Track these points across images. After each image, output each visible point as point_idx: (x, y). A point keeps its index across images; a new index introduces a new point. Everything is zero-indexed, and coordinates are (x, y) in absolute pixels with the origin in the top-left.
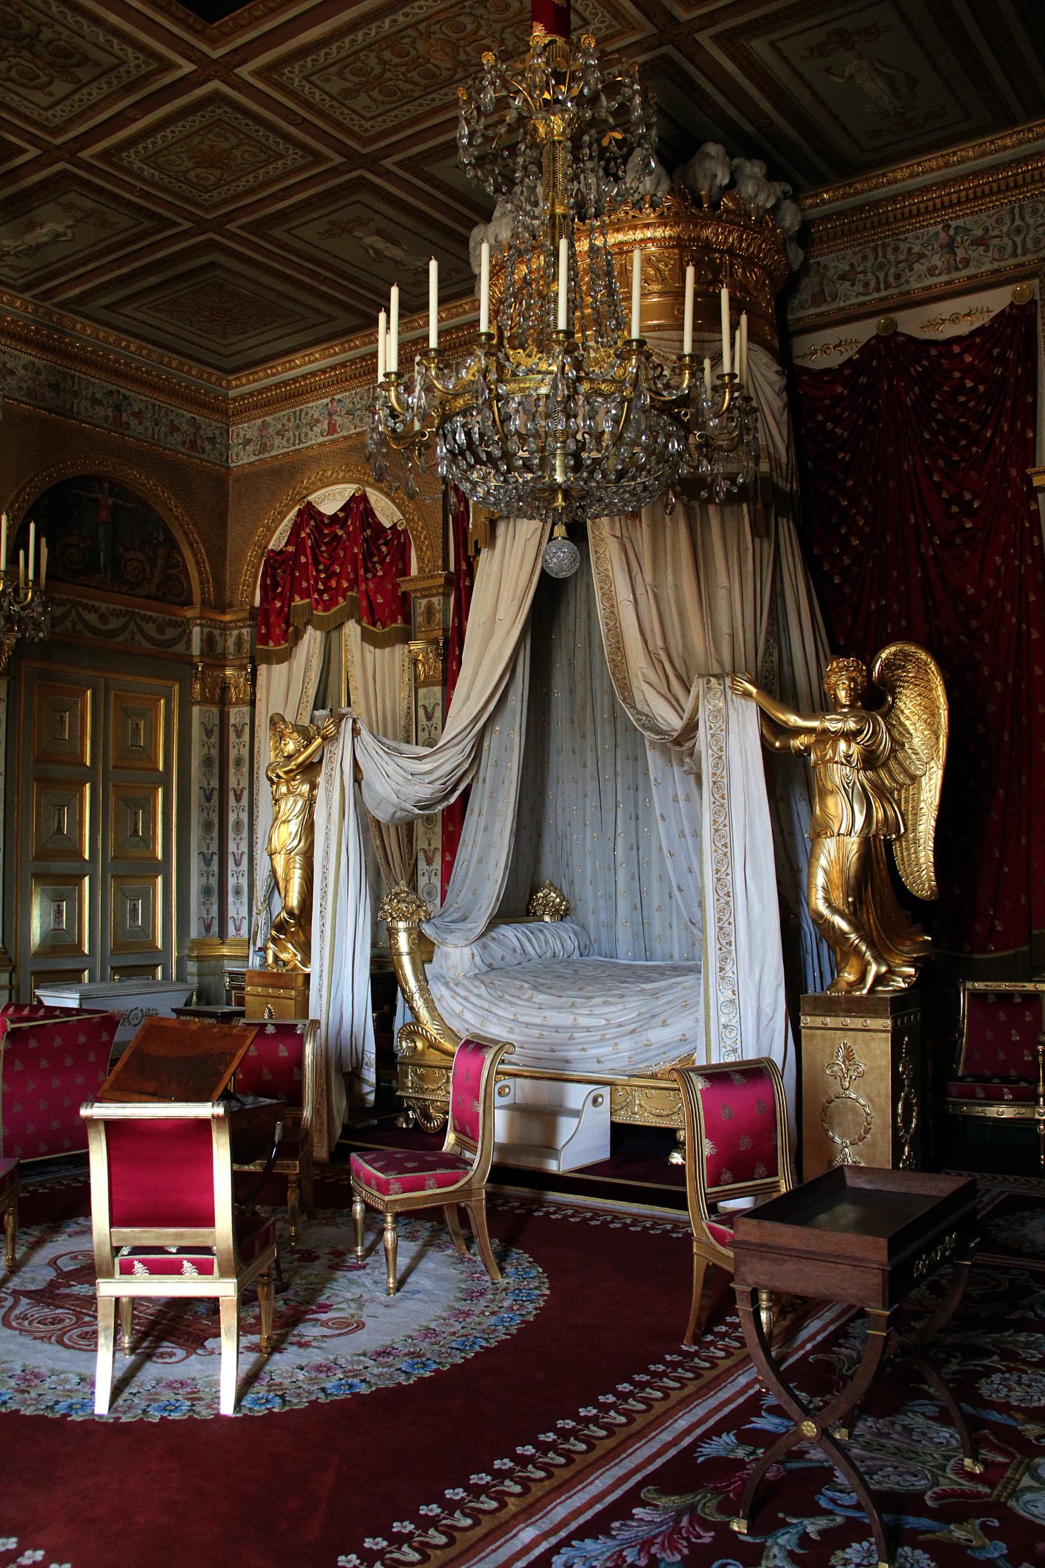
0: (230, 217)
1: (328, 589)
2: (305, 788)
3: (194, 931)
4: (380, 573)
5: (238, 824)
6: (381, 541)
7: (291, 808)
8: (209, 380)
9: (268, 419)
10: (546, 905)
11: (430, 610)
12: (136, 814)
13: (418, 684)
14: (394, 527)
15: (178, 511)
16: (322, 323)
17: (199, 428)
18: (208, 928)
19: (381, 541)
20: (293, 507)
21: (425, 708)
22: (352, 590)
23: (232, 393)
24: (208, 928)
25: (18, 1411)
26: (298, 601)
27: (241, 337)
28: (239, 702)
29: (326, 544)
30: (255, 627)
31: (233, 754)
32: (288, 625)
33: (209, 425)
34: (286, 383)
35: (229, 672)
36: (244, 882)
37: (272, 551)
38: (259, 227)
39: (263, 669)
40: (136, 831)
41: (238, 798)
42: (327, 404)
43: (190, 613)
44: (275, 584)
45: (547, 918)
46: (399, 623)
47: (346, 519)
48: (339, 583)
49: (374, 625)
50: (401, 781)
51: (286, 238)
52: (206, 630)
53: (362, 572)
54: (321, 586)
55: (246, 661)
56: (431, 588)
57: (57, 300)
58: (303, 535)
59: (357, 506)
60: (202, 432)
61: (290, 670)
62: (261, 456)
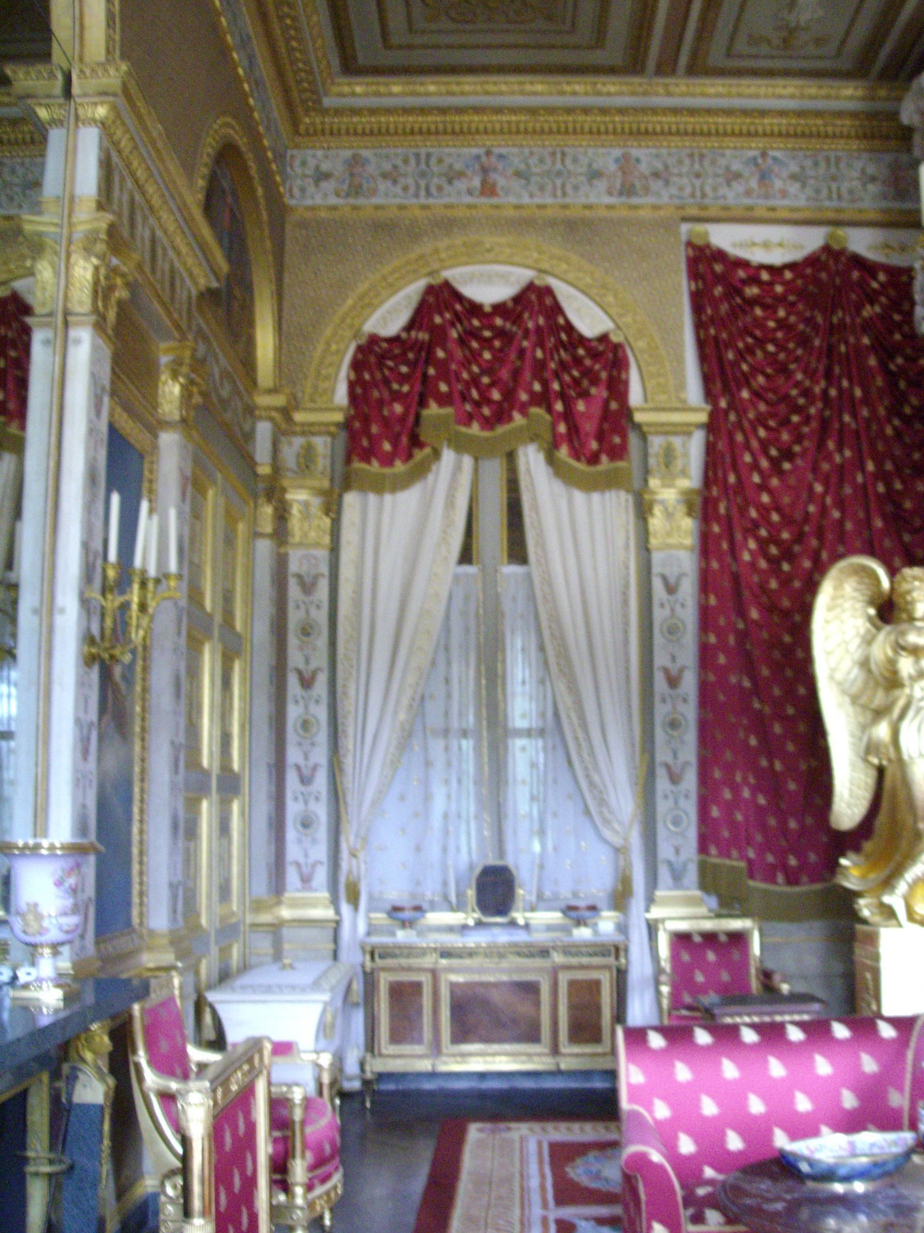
11: (669, 455)
21: (664, 578)
42: (478, 157)
54: (475, 394)
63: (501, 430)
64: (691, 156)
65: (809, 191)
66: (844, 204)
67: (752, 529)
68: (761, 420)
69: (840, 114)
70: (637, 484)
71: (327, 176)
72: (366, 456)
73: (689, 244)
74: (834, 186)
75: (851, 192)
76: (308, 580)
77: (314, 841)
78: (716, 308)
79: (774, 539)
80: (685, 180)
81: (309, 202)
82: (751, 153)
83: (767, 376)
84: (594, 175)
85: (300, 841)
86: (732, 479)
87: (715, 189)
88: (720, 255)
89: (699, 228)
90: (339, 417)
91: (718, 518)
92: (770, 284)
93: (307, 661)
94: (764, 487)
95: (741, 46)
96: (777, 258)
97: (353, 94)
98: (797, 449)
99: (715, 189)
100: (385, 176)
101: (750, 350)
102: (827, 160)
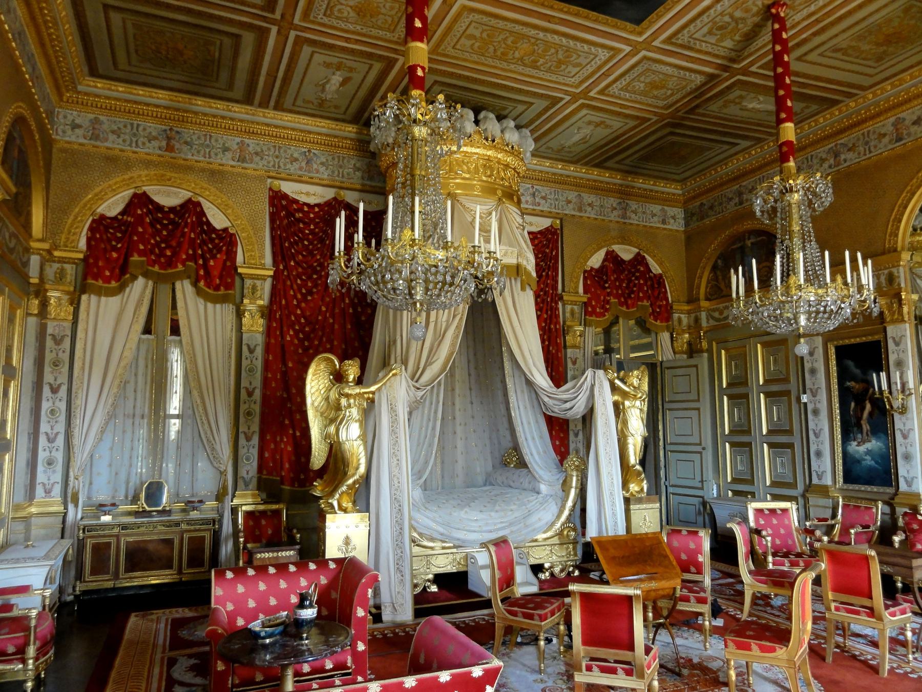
11: (254, 288)
14: (225, 230)
21: (248, 346)
22: (191, 261)
26: (135, 258)
39: (84, 297)
42: (165, 130)
49: (209, 288)
63: (170, 271)
64: (275, 147)
65: (329, 172)
66: (344, 180)
67: (292, 326)
68: (299, 276)
69: (346, 138)
70: (238, 300)
71: (79, 126)
72: (96, 278)
73: (270, 189)
74: (341, 171)
75: (348, 174)
76: (58, 338)
77: (54, 472)
78: (281, 221)
79: (302, 330)
80: (271, 158)
81: (67, 139)
82: (304, 150)
83: (303, 255)
84: (226, 149)
86: (284, 302)
87: (285, 165)
88: (285, 196)
89: (276, 182)
90: (81, 256)
91: (275, 320)
92: (308, 212)
93: (55, 380)
94: (298, 306)
95: (299, 102)
96: (312, 201)
97: (96, 87)
98: (315, 290)
99: (285, 165)
100: (113, 132)
101: (296, 243)
102: (339, 157)
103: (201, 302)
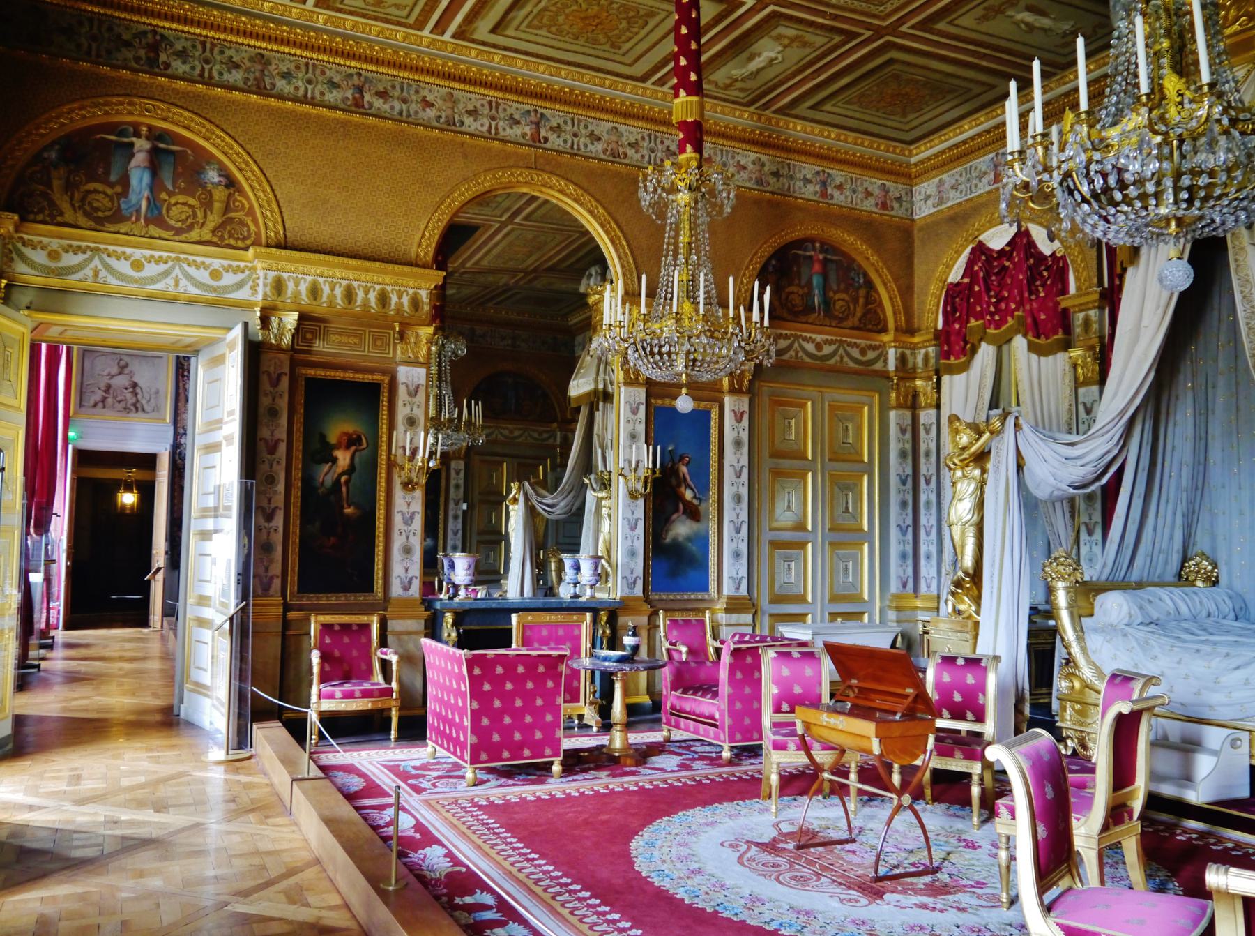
0: (901, 21)
1: (998, 311)
2: (977, 472)
3: (894, 587)
4: (1042, 294)
5: (928, 503)
6: (1043, 268)
7: (967, 489)
8: (894, 152)
9: (944, 176)
10: (1198, 572)
12: (847, 495)
13: (1077, 384)
14: (1053, 254)
15: (874, 259)
16: (985, 92)
17: (887, 192)
18: (904, 585)
19: (1043, 268)
20: (967, 246)
21: (1084, 404)
23: (913, 160)
24: (904, 585)
25: (745, 921)
26: (973, 323)
27: (917, 114)
28: (928, 406)
29: (996, 274)
30: (940, 345)
31: (923, 447)
32: (966, 343)
33: (896, 188)
34: (957, 146)
35: (919, 383)
36: (934, 549)
37: (951, 284)
38: (925, 25)
39: (946, 379)
40: (847, 508)
41: (928, 482)
43: (887, 338)
44: (954, 310)
45: (1199, 583)
46: (1060, 335)
47: (1011, 252)
48: (1007, 305)
49: (1038, 337)
50: (1056, 464)
51: (952, 30)
52: (899, 351)
53: (1026, 295)
54: (992, 309)
55: (932, 373)
56: (1088, 303)
57: (773, 108)
58: (976, 268)
59: (1022, 241)
60: (891, 194)
61: (968, 379)
62: (940, 208)
85: (926, 566)
100: (952, 188)
103: (1034, 357)
